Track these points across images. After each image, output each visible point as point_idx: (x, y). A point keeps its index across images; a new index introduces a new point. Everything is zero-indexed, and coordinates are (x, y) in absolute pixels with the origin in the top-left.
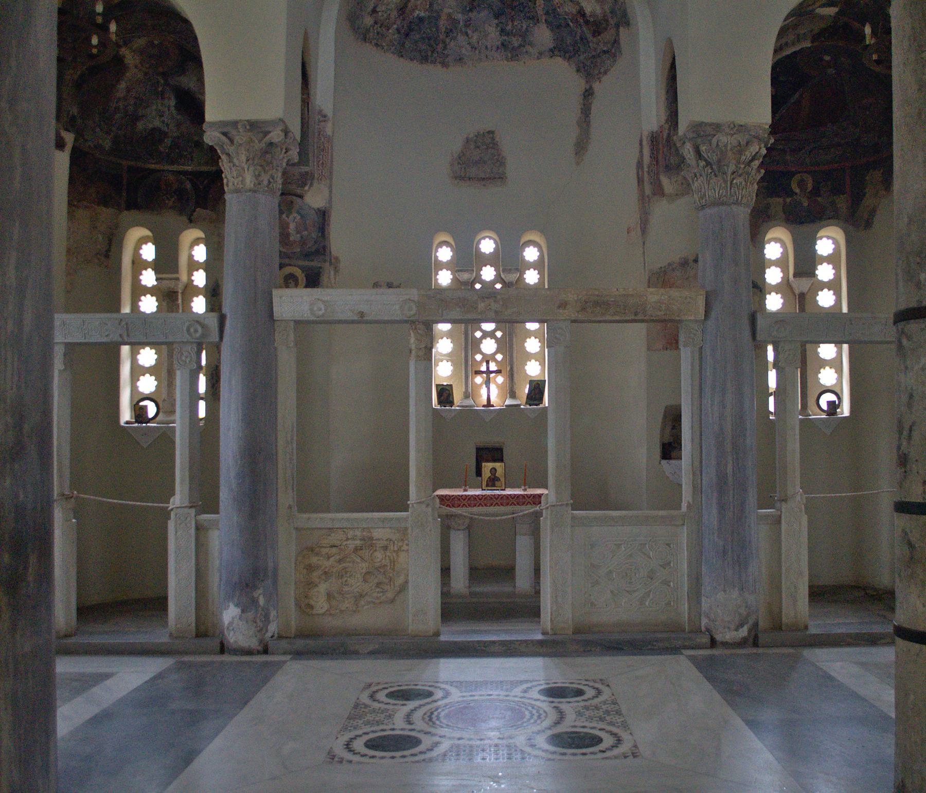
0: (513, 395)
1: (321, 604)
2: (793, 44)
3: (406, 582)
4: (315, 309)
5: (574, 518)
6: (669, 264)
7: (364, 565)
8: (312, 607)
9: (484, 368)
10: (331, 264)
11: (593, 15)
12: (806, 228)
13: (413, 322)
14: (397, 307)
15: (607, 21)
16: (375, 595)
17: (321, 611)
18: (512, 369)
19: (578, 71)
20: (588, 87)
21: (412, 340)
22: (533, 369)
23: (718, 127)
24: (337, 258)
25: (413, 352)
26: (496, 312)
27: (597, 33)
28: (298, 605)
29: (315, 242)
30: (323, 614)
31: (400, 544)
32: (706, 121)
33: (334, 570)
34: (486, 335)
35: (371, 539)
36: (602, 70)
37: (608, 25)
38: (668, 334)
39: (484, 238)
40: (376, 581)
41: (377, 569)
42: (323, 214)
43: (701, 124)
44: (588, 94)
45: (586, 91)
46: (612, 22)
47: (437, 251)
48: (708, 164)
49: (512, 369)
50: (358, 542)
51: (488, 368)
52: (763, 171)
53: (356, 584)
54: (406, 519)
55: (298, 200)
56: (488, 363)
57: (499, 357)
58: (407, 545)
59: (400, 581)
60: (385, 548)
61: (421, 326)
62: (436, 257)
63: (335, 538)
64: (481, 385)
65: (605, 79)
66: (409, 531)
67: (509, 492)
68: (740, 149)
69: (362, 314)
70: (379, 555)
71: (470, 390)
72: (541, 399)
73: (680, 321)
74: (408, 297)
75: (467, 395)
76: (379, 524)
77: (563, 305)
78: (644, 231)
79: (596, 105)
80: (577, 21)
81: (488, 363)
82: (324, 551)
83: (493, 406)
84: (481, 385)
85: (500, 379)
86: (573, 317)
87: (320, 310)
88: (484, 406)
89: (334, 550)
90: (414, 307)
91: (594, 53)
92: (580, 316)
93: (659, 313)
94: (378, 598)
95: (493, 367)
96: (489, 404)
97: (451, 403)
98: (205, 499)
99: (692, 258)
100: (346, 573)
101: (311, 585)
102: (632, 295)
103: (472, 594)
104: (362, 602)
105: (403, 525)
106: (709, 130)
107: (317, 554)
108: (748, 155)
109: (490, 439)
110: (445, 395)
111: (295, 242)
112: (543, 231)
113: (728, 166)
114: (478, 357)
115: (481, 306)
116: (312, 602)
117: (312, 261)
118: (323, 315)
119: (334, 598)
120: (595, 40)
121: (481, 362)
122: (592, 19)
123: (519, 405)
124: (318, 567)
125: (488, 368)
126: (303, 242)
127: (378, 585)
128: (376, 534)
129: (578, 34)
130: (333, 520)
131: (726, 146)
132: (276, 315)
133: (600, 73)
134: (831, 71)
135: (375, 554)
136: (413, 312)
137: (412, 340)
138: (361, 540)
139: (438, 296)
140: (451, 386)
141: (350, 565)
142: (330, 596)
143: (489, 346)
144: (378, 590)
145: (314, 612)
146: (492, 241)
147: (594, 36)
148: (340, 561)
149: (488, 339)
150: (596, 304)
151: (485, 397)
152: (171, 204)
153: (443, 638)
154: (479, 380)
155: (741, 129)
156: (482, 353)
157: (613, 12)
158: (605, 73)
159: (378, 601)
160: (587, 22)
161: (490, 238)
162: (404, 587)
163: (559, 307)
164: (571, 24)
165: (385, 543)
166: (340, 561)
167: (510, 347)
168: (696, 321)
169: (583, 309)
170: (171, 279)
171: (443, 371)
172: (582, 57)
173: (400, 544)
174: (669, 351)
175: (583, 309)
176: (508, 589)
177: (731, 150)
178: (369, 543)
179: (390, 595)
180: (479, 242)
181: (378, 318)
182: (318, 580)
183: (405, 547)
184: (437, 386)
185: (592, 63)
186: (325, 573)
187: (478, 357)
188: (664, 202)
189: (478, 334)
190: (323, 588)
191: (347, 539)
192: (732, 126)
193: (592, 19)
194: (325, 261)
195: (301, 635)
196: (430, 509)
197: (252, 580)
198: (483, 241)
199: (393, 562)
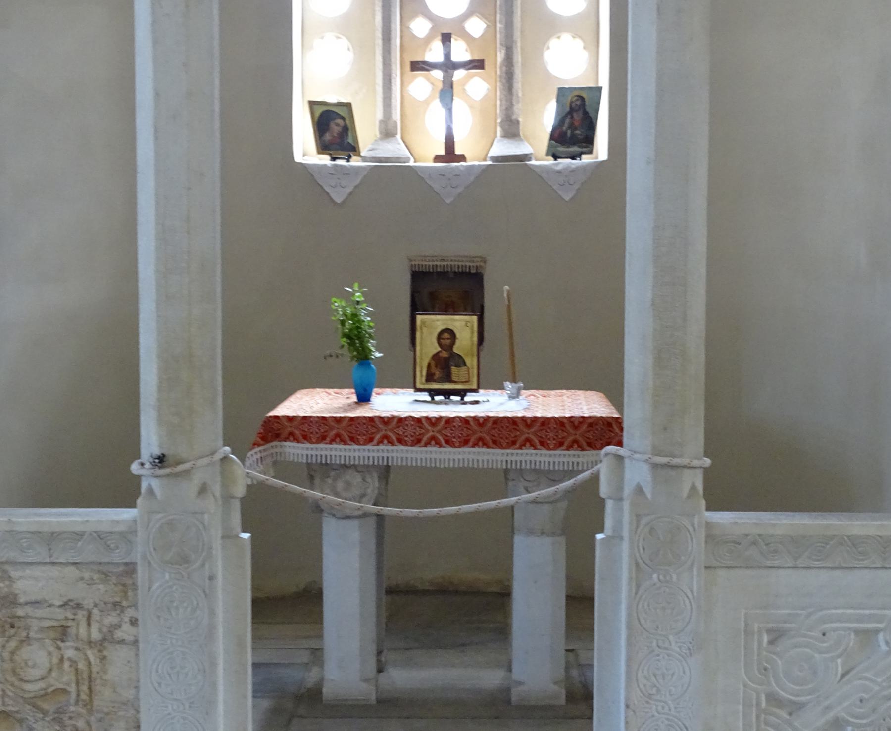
0: (511, 130)
5: (713, 537)
9: (435, 53)
41: (33, 702)
51: (447, 56)
54: (127, 535)
56: (446, 38)
57: (476, 27)
58: (134, 622)
60: (62, 632)
66: (141, 573)
67: (494, 403)
70: (38, 657)
71: (396, 116)
72: (588, 142)
75: (387, 132)
81: (446, 38)
83: (462, 158)
84: (427, 102)
85: (476, 87)
88: (438, 158)
95: (460, 52)
96: (450, 154)
97: (352, 149)
103: (388, 704)
105: (118, 557)
109: (449, 249)
110: (335, 128)
121: (428, 40)
125: (447, 56)
135: (25, 653)
140: (348, 106)
154: (422, 87)
165: (60, 614)
173: (111, 619)
176: (490, 678)
184: (312, 104)
187: (420, 27)
196: (212, 506)
199: (88, 681)
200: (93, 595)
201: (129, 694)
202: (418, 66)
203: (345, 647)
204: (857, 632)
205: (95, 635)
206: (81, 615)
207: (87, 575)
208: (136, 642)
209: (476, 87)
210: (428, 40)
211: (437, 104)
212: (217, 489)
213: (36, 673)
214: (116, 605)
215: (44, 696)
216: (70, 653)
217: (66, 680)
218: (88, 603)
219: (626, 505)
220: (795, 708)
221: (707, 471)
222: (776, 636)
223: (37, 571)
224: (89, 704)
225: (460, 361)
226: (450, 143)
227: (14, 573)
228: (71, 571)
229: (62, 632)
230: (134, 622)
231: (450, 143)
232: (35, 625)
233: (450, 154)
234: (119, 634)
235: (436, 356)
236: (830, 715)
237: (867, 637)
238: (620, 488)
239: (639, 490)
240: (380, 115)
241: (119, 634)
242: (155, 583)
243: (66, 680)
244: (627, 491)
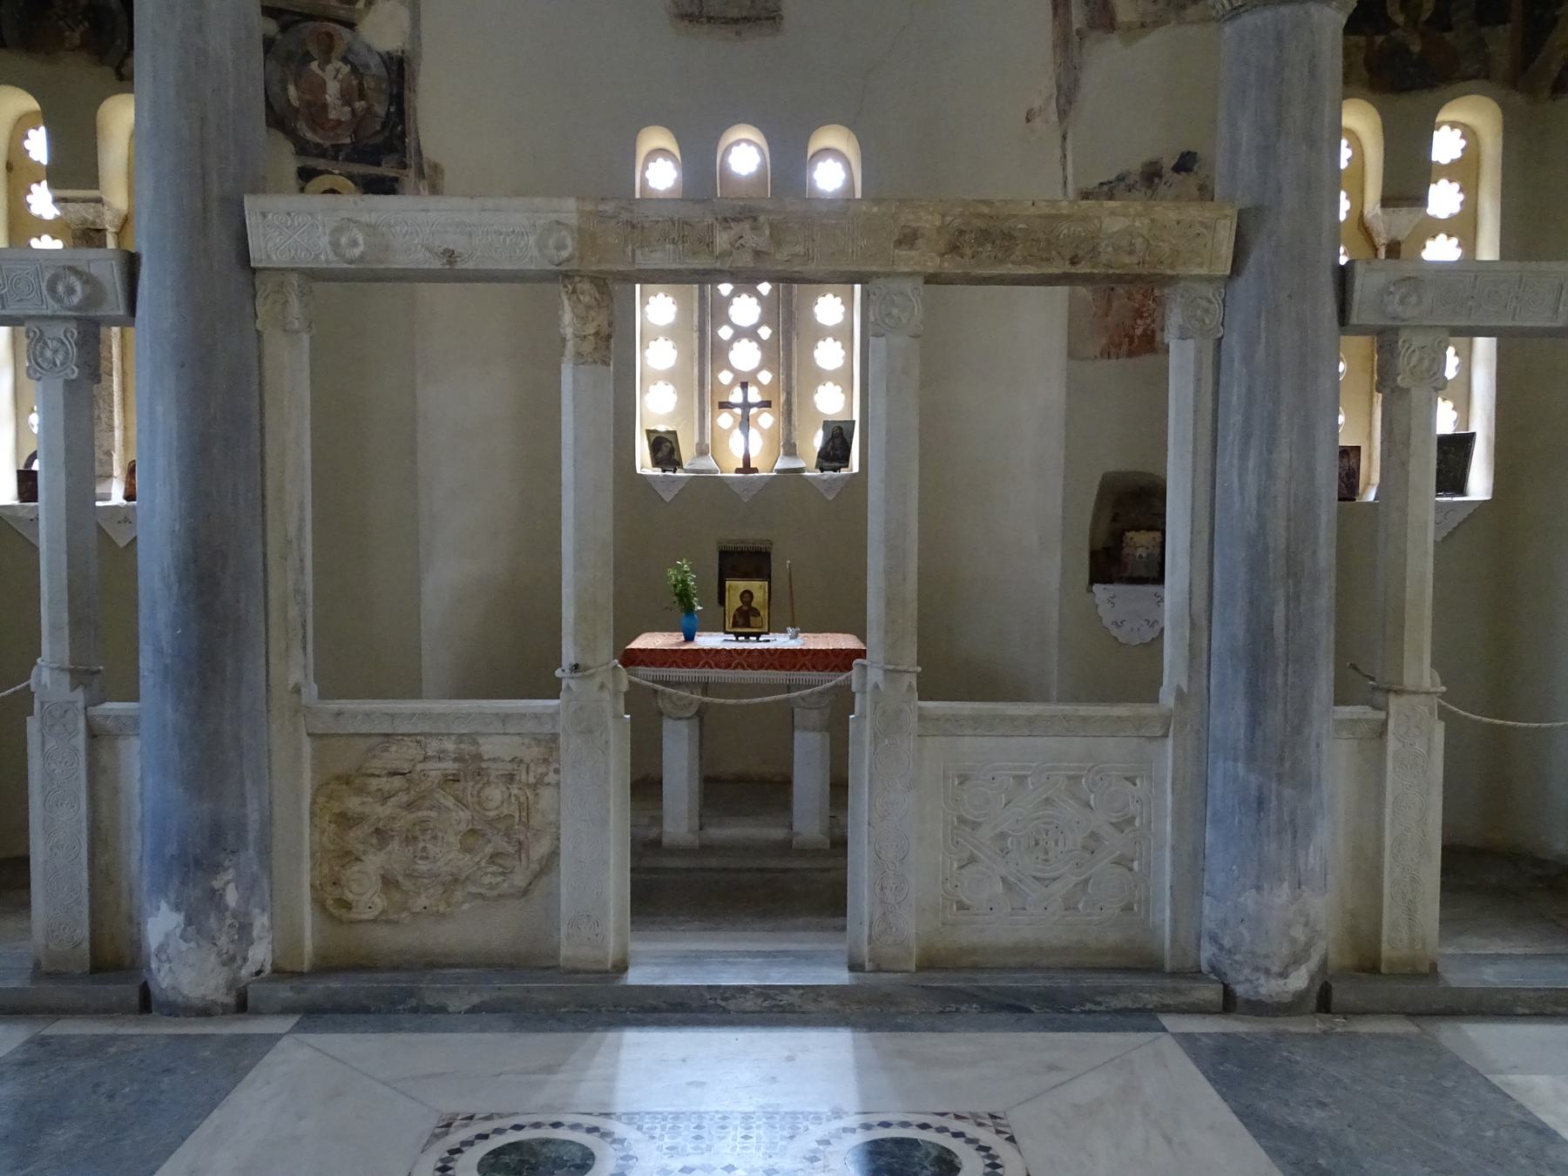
0: (791, 450)
1: (368, 897)
3: (555, 854)
4: (344, 240)
5: (922, 717)
6: (1120, 178)
7: (465, 815)
8: (348, 906)
9: (736, 396)
10: (420, 173)
12: (1405, 103)
13: (567, 276)
14: (532, 239)
16: (487, 880)
17: (369, 915)
18: (789, 402)
21: (568, 317)
22: (831, 402)
24: (436, 168)
25: (570, 345)
26: (757, 254)
28: (319, 904)
29: (384, 125)
30: (374, 921)
31: (541, 770)
33: (397, 825)
34: (740, 333)
35: (478, 757)
38: (1125, 316)
39: (738, 143)
40: (489, 849)
41: (490, 823)
42: (398, 70)
47: (645, 168)
49: (789, 402)
50: (450, 766)
51: (745, 397)
53: (447, 856)
54: (554, 716)
55: (345, 33)
56: (744, 386)
57: (765, 377)
58: (557, 771)
59: (540, 849)
60: (510, 778)
61: (586, 286)
62: (644, 181)
63: (396, 756)
64: (730, 430)
66: (562, 739)
67: (781, 641)
69: (450, 255)
71: (708, 441)
72: (845, 460)
73: (1171, 280)
74: (554, 217)
75: (702, 452)
76: (501, 724)
77: (909, 239)
78: (1063, 114)
81: (744, 386)
82: (374, 783)
83: (755, 470)
84: (730, 430)
85: (766, 419)
86: (931, 266)
87: (355, 243)
88: (738, 471)
89: (397, 782)
90: (569, 242)
92: (949, 266)
93: (1127, 260)
94: (491, 887)
95: (754, 395)
96: (747, 467)
98: (102, 669)
99: (1169, 162)
100: (424, 831)
101: (348, 857)
102: (1068, 217)
103: (707, 849)
104: (459, 895)
105: (547, 729)
107: (361, 791)
109: (748, 534)
110: (665, 449)
111: (339, 123)
112: (852, 125)
114: (725, 377)
115: (722, 240)
116: (350, 897)
117: (379, 164)
118: (362, 258)
119: (397, 885)
121: (731, 386)
123: (801, 470)
124: (359, 819)
125: (745, 397)
126: (358, 123)
127: (494, 858)
128: (488, 747)
130: (393, 716)
132: (257, 257)
135: (487, 791)
136: (565, 254)
137: (568, 317)
138: (455, 760)
139: (625, 216)
140: (674, 433)
141: (433, 814)
142: (388, 882)
143: (745, 356)
144: (494, 868)
145: (353, 915)
146: (753, 149)
148: (409, 806)
149: (745, 341)
150: (984, 236)
151: (740, 455)
152: (77, 41)
153: (634, 977)
154: (725, 420)
156: (732, 370)
159: (495, 893)
161: (749, 142)
162: (551, 861)
163: (899, 243)
165: (509, 767)
166: (409, 806)
167: (788, 337)
168: (1210, 279)
169: (954, 248)
170: (85, 201)
171: (657, 405)
173: (541, 770)
174: (1113, 361)
175: (954, 248)
176: (778, 833)
178: (471, 768)
179: (519, 880)
180: (728, 150)
181: (490, 265)
182: (361, 847)
183: (551, 778)
184: (649, 432)
186: (378, 831)
187: (725, 377)
188: (1114, 43)
189: (725, 333)
190: (374, 862)
191: (426, 758)
194: (404, 166)
195: (324, 968)
196: (606, 695)
197: (200, 858)
198: (735, 149)
199: (525, 809)
200: (533, 753)
201: (552, 817)
202: (725, 405)
203: (679, 814)
204: (1015, 777)
205: (532, 780)
206: (523, 767)
207: (526, 741)
208: (558, 784)
209: (766, 419)
210: (731, 386)
211: (737, 433)
212: (610, 686)
213: (493, 804)
214: (545, 760)
215: (499, 819)
216: (515, 791)
217: (513, 809)
218: (527, 759)
219: (868, 696)
220: (975, 825)
221: (919, 676)
222: (964, 779)
223: (495, 739)
224: (527, 825)
225: (756, 613)
226: (747, 460)
227: (481, 740)
228: (517, 739)
229: (510, 778)
230: (557, 771)
231: (747, 460)
232: (494, 774)
233: (747, 467)
234: (547, 779)
235: (739, 609)
236: (998, 830)
237: (1021, 780)
238: (864, 684)
239: (876, 686)
240: (696, 440)
241: (547, 779)
242: (570, 745)
243: (513, 809)
244: (869, 687)
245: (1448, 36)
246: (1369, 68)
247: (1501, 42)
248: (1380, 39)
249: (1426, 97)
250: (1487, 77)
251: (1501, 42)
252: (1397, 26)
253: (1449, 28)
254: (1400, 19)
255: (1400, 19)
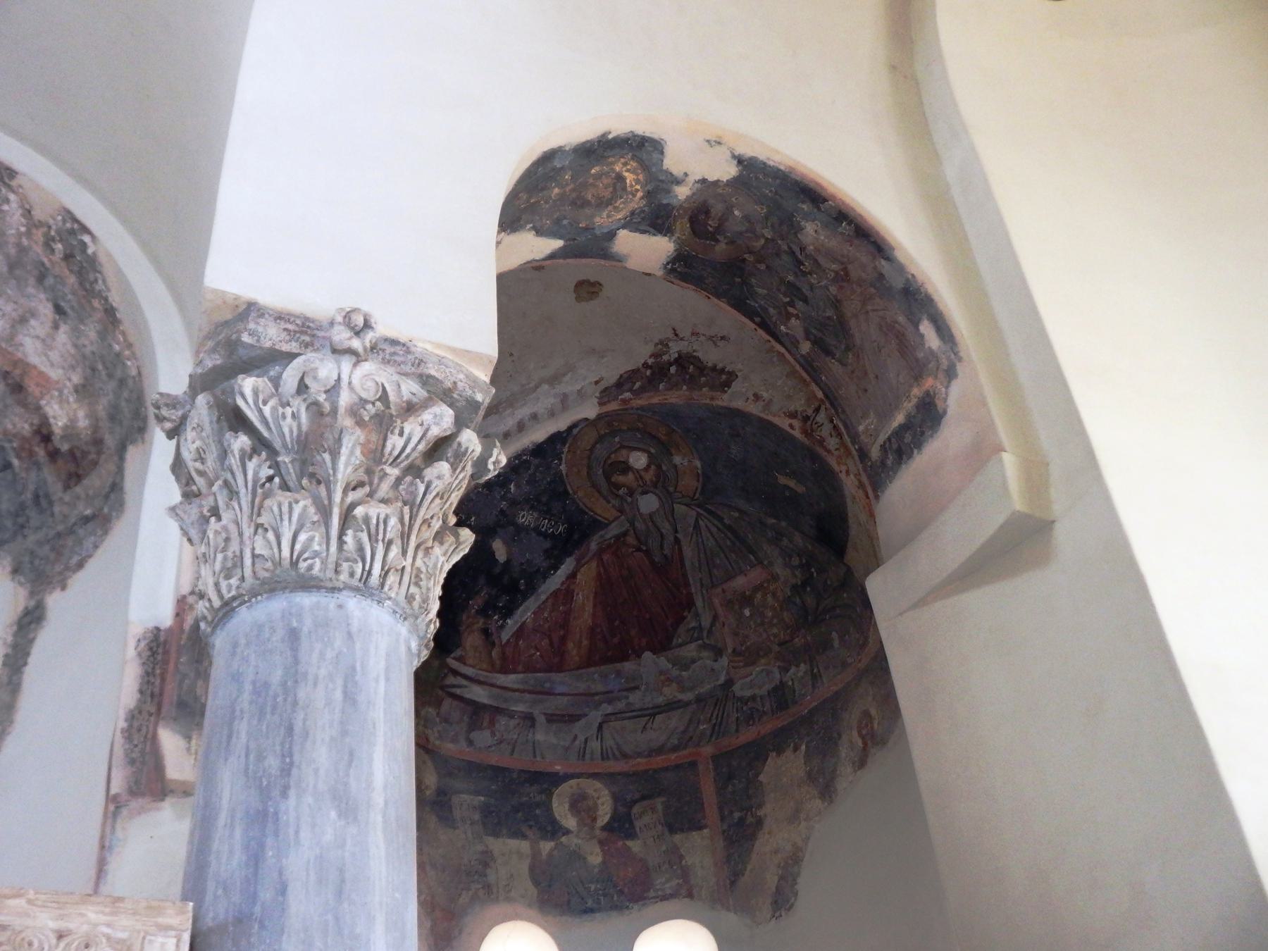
2: (552, 414)
11: (70, 431)
15: (98, 442)
19: (16, 571)
20: (32, 603)
23: (307, 331)
27: (74, 479)
32: (266, 298)
36: (75, 559)
37: (99, 453)
43: (249, 310)
44: (31, 620)
45: (27, 612)
46: (110, 441)
48: (261, 444)
52: (468, 536)
65: (79, 581)
68: (383, 417)
79: (45, 643)
80: (31, 454)
91: (60, 528)
106: (271, 335)
108: (412, 435)
113: (335, 455)
120: (67, 498)
122: (65, 447)
129: (31, 487)
131: (333, 390)
133: (67, 568)
134: (648, 503)
147: (67, 487)
155: (392, 351)
157: (113, 417)
158: (80, 565)
160: (54, 455)
164: (16, 462)
172: (32, 538)
177: (353, 412)
185: (53, 549)
192: (360, 321)
193: (65, 447)
245: (635, 846)
246: (536, 883)
247: (700, 850)
248: (547, 846)
249: (617, 922)
250: (690, 895)
251: (700, 850)
252: (567, 832)
253: (631, 835)
254: (570, 822)
255: (570, 822)
